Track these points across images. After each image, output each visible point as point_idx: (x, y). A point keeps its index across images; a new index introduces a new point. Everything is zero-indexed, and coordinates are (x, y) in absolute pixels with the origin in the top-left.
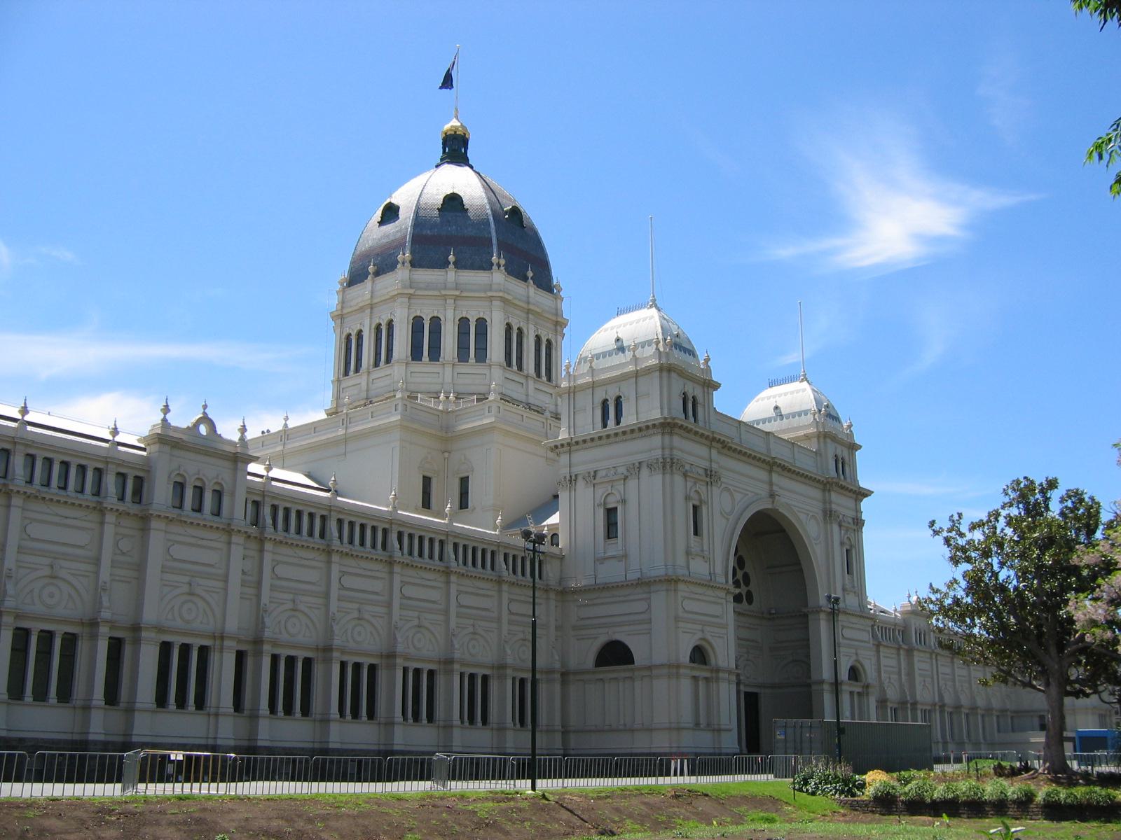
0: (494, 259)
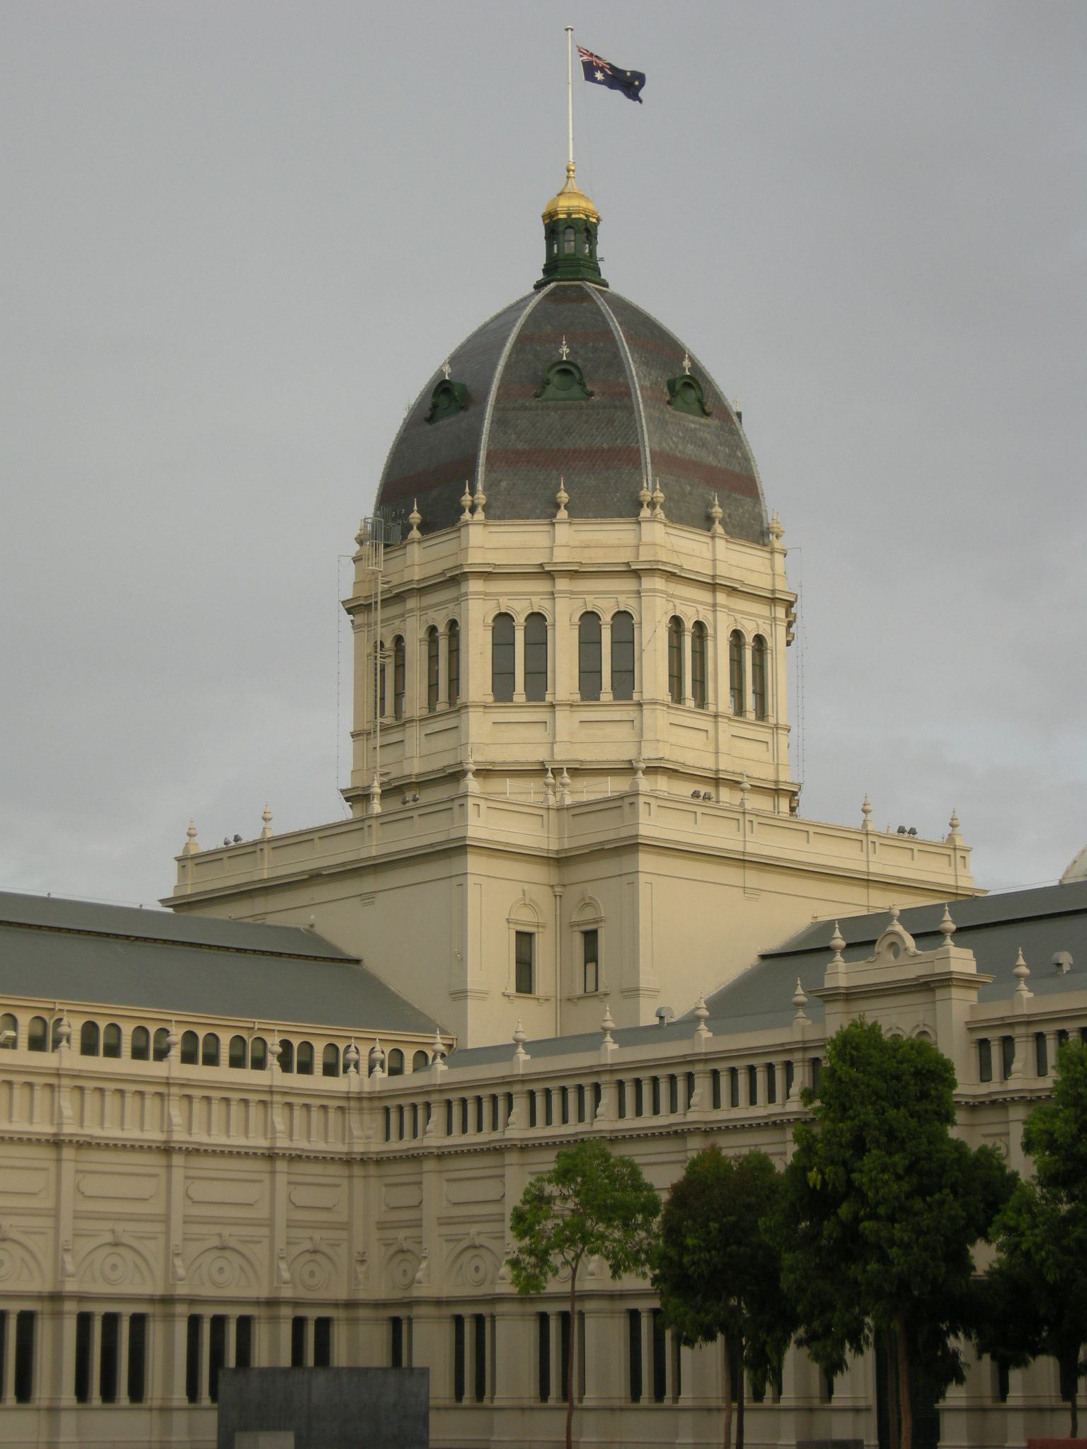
0: (646, 495)
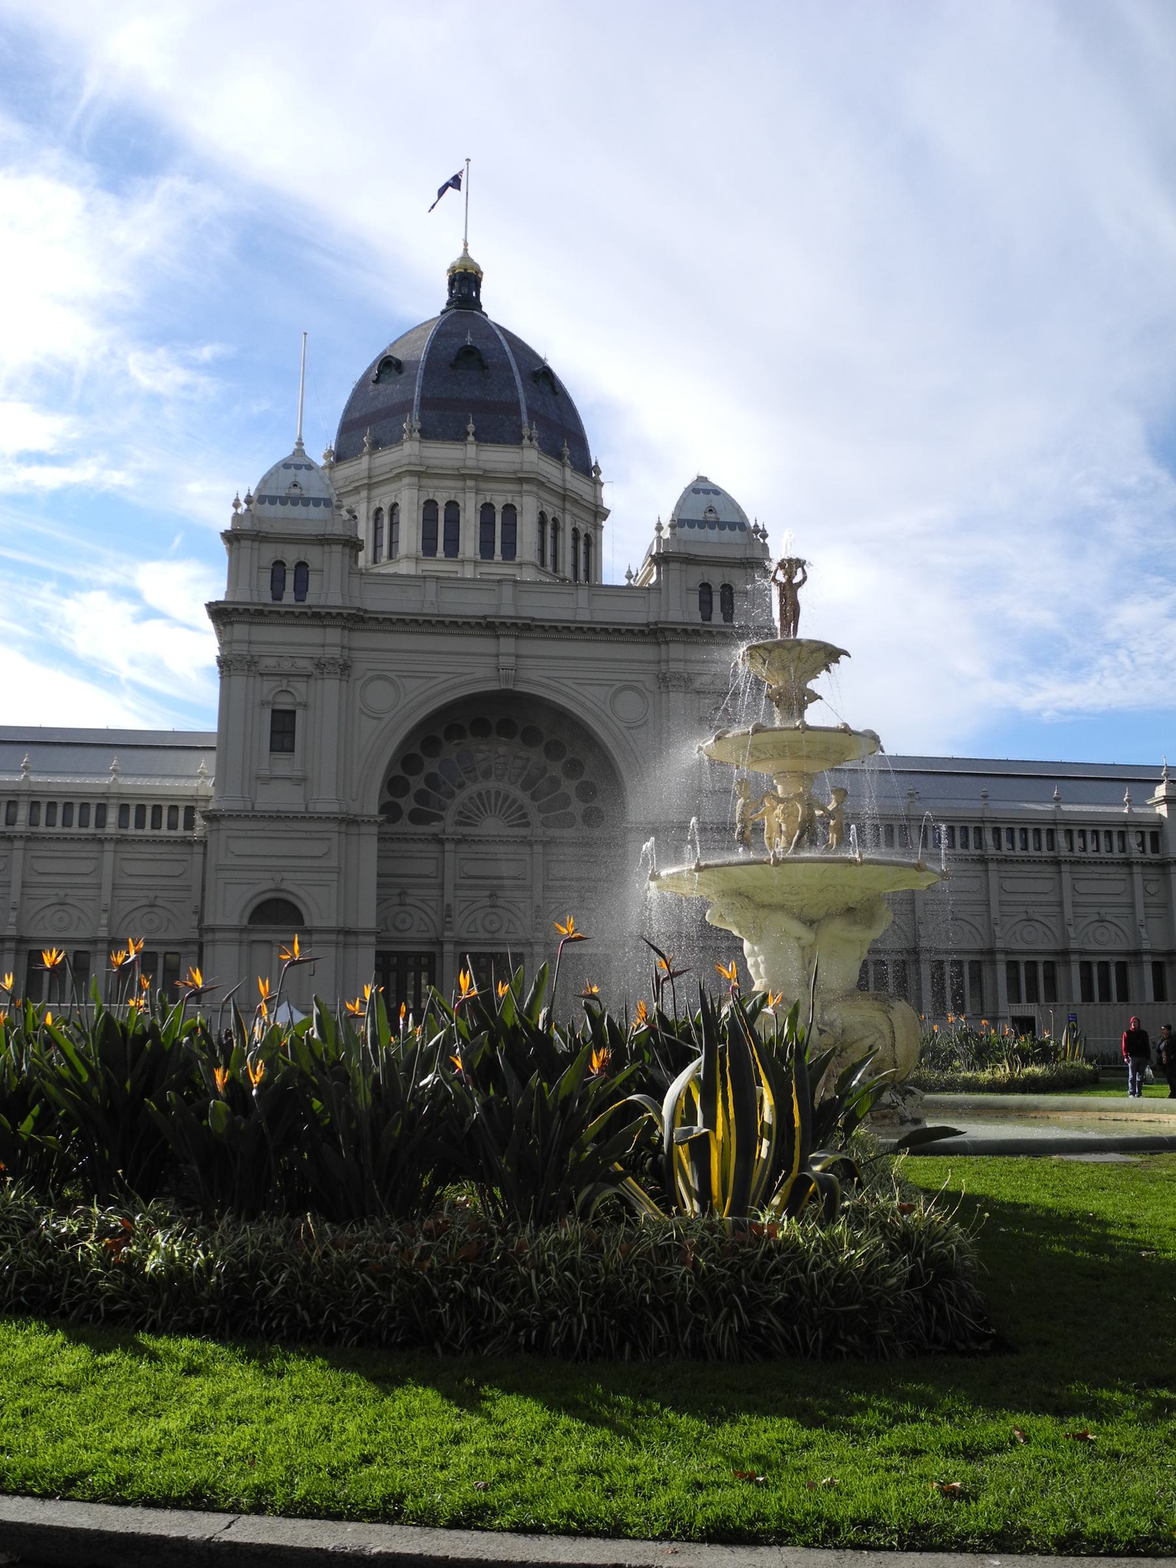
0: (526, 432)
